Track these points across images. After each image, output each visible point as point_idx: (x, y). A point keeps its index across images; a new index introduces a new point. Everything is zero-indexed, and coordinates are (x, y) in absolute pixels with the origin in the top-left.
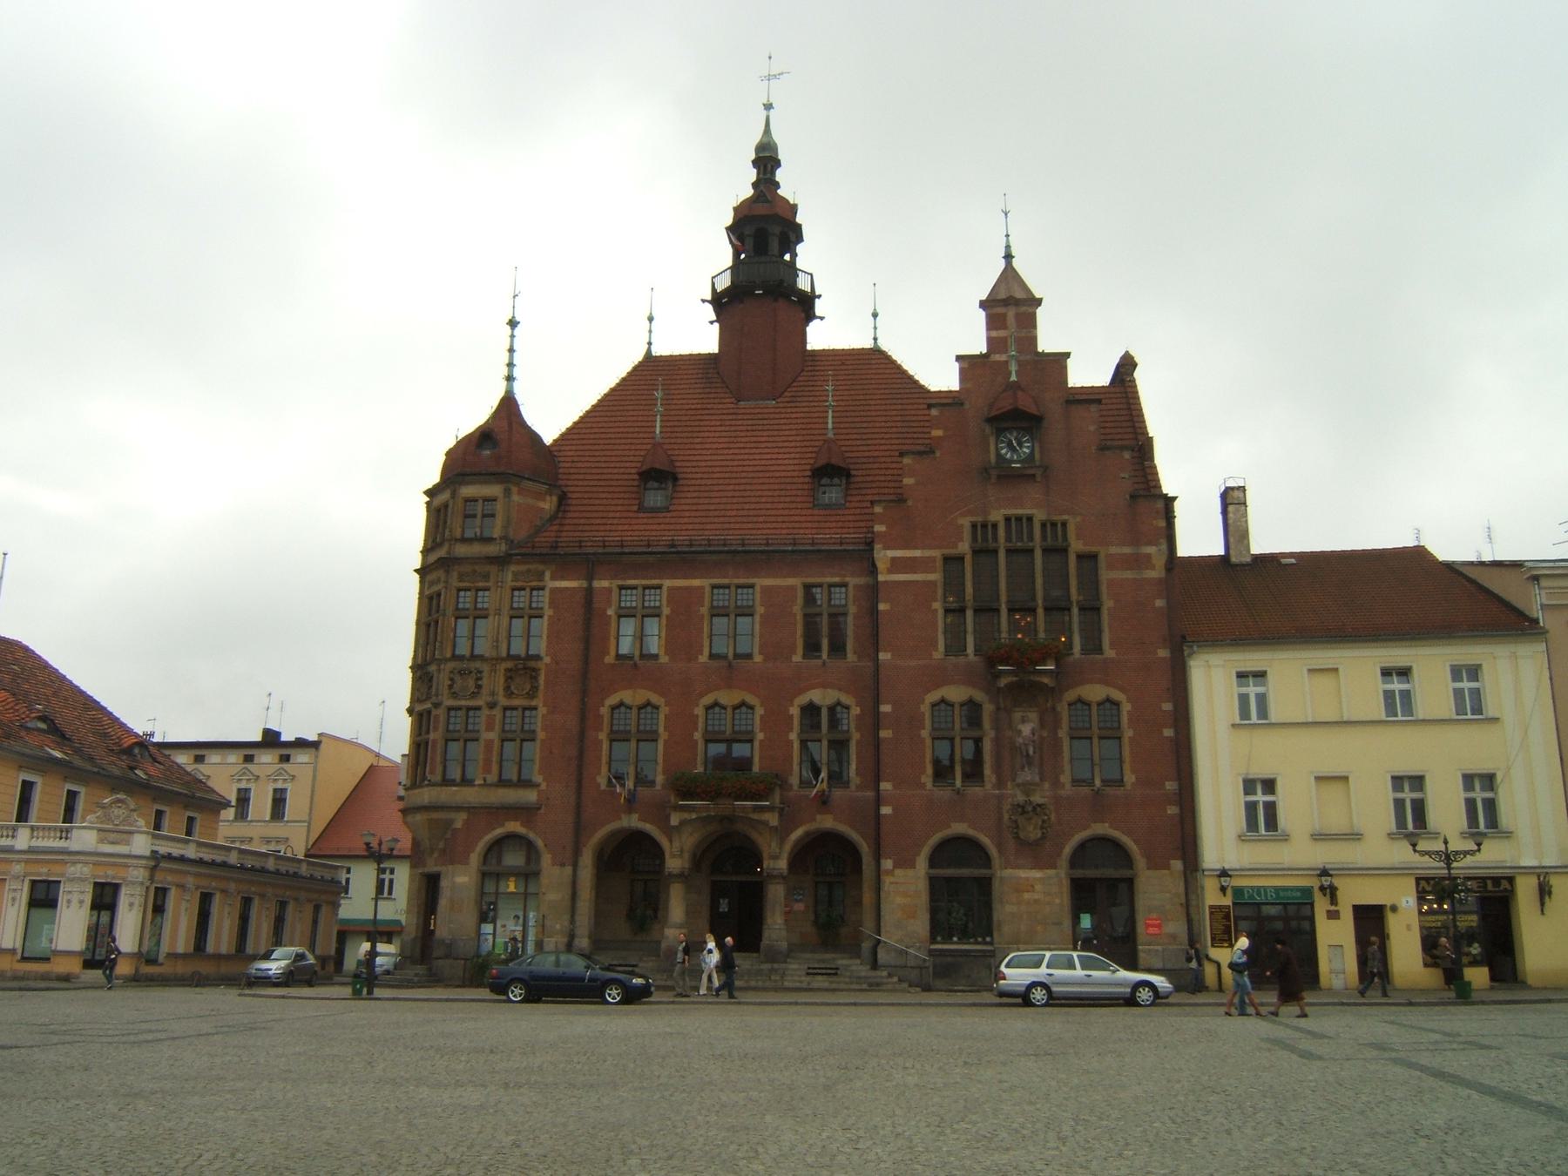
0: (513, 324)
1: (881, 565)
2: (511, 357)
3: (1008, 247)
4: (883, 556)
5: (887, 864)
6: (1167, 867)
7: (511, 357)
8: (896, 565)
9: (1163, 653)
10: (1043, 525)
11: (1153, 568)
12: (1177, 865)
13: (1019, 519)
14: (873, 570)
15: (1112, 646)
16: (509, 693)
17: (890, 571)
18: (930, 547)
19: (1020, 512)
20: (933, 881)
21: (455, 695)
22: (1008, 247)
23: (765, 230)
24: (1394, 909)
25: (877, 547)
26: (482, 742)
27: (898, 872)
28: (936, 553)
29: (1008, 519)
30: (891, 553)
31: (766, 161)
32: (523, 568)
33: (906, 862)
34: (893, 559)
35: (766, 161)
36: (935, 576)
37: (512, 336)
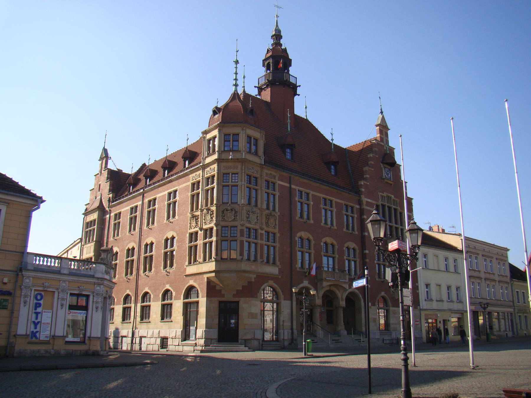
0: (237, 62)
1: (364, 203)
2: (236, 76)
3: (381, 109)
4: (365, 199)
7: (236, 76)
8: (368, 204)
14: (360, 203)
16: (267, 224)
18: (374, 200)
19: (389, 195)
21: (250, 222)
22: (381, 109)
23: (278, 62)
24: (449, 320)
25: (363, 196)
26: (238, 241)
28: (374, 202)
30: (366, 199)
31: (277, 36)
32: (269, 172)
35: (277, 36)
37: (236, 68)
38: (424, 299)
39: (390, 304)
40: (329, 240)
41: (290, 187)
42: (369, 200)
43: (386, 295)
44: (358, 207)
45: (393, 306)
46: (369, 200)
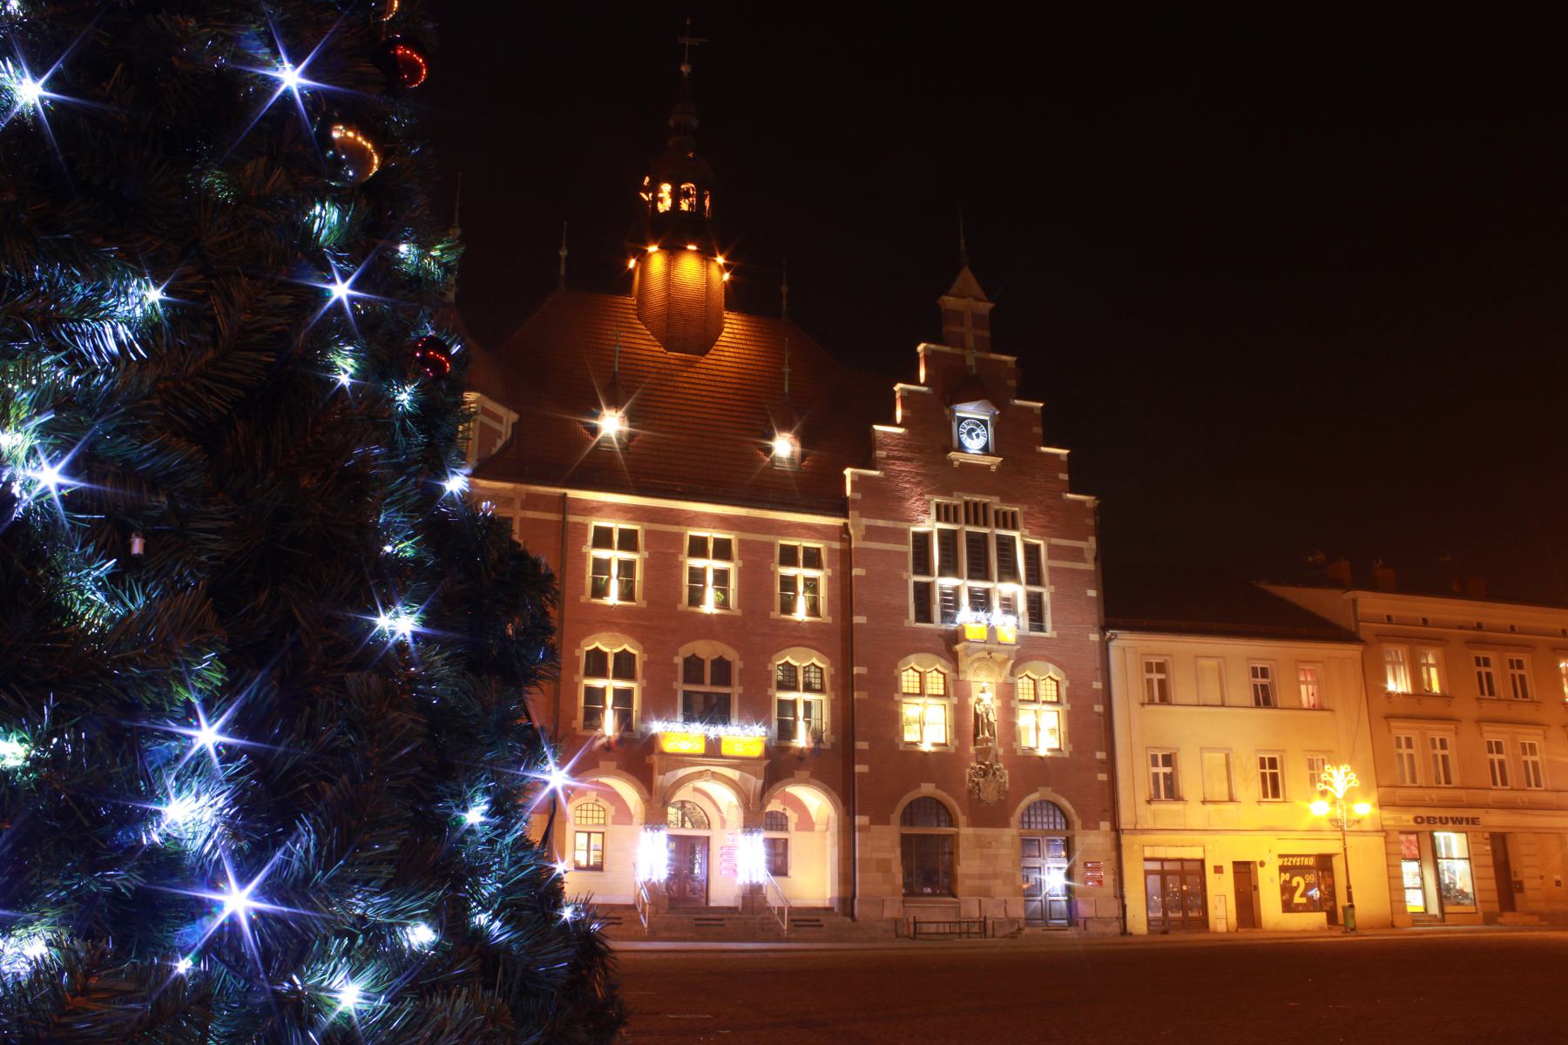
5: (860, 820)
6: (1097, 827)
9: (1094, 637)
10: (996, 512)
11: (1084, 561)
12: (1105, 826)
13: (976, 504)
15: (1054, 628)
17: (865, 538)
19: (977, 499)
20: (905, 839)
24: (1262, 864)
27: (874, 828)
29: (966, 503)
30: (865, 521)
33: (880, 819)
34: (868, 528)
36: (910, 548)
38: (1142, 796)
39: (962, 819)
40: (706, 650)
41: (564, 522)
42: (881, 523)
43: (941, 794)
44: (837, 545)
45: (975, 822)
46: (881, 523)
